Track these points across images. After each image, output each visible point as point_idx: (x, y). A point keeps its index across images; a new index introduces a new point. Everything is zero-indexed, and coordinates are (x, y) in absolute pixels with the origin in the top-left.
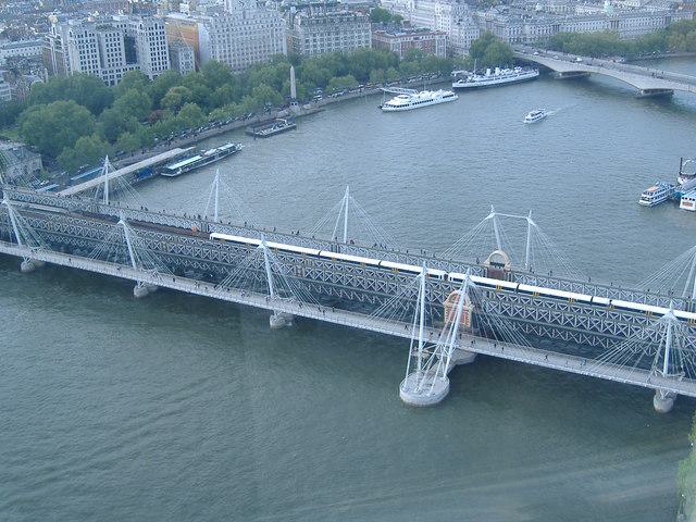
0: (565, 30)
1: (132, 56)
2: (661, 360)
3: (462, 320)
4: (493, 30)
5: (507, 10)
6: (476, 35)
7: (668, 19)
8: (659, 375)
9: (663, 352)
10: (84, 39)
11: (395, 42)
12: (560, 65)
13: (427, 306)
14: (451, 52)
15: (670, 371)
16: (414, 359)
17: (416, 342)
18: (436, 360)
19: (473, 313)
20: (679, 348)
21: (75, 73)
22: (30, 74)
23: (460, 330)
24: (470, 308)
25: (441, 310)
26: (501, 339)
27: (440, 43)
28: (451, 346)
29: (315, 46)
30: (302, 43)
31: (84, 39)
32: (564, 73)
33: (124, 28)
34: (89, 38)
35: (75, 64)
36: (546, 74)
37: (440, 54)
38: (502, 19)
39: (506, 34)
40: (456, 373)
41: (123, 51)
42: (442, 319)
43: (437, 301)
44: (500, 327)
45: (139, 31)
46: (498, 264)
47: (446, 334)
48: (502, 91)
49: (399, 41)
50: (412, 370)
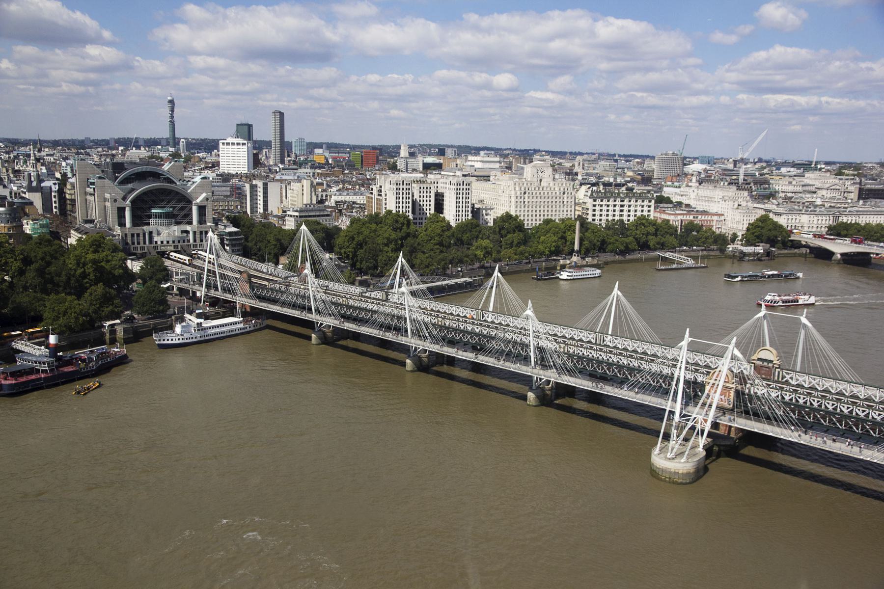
0: (845, 221)
1: (439, 206)
4: (771, 216)
10: (401, 187)
11: (675, 218)
12: (840, 247)
21: (390, 212)
22: (352, 212)
29: (601, 215)
30: (590, 212)
31: (401, 187)
33: (436, 184)
34: (405, 187)
35: (391, 206)
41: (433, 203)
45: (448, 186)
49: (680, 217)
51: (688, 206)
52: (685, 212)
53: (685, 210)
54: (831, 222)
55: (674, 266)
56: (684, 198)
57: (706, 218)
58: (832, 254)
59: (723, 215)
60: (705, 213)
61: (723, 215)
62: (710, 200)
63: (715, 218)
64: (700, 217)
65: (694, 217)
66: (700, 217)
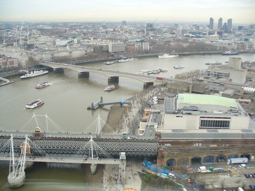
0: (55, 56)
2: (91, 154)
3: (27, 151)
4: (33, 56)
5: (37, 50)
6: (27, 59)
7: (86, 51)
8: (91, 159)
9: (91, 152)
13: (14, 149)
14: (19, 65)
15: (94, 157)
16: (12, 167)
17: (12, 161)
18: (20, 166)
19: (30, 149)
20: (96, 150)
23: (27, 155)
24: (30, 147)
25: (20, 149)
26: (40, 156)
27: (15, 61)
28: (24, 161)
32: (56, 69)
36: (50, 70)
37: (16, 65)
38: (35, 53)
39: (37, 58)
40: (28, 170)
42: (21, 152)
43: (18, 147)
44: (40, 152)
46: (38, 132)
47: (22, 157)
48: (37, 78)
50: (12, 171)
51: (4, 55)
52: (3, 59)
53: (2, 58)
54: (51, 56)
55: (3, 84)
56: (2, 51)
57: (11, 60)
58: (53, 69)
59: (17, 58)
60: (10, 58)
61: (17, 58)
62: (12, 52)
63: (14, 60)
64: (9, 60)
65: (7, 60)
66: (9, 60)
